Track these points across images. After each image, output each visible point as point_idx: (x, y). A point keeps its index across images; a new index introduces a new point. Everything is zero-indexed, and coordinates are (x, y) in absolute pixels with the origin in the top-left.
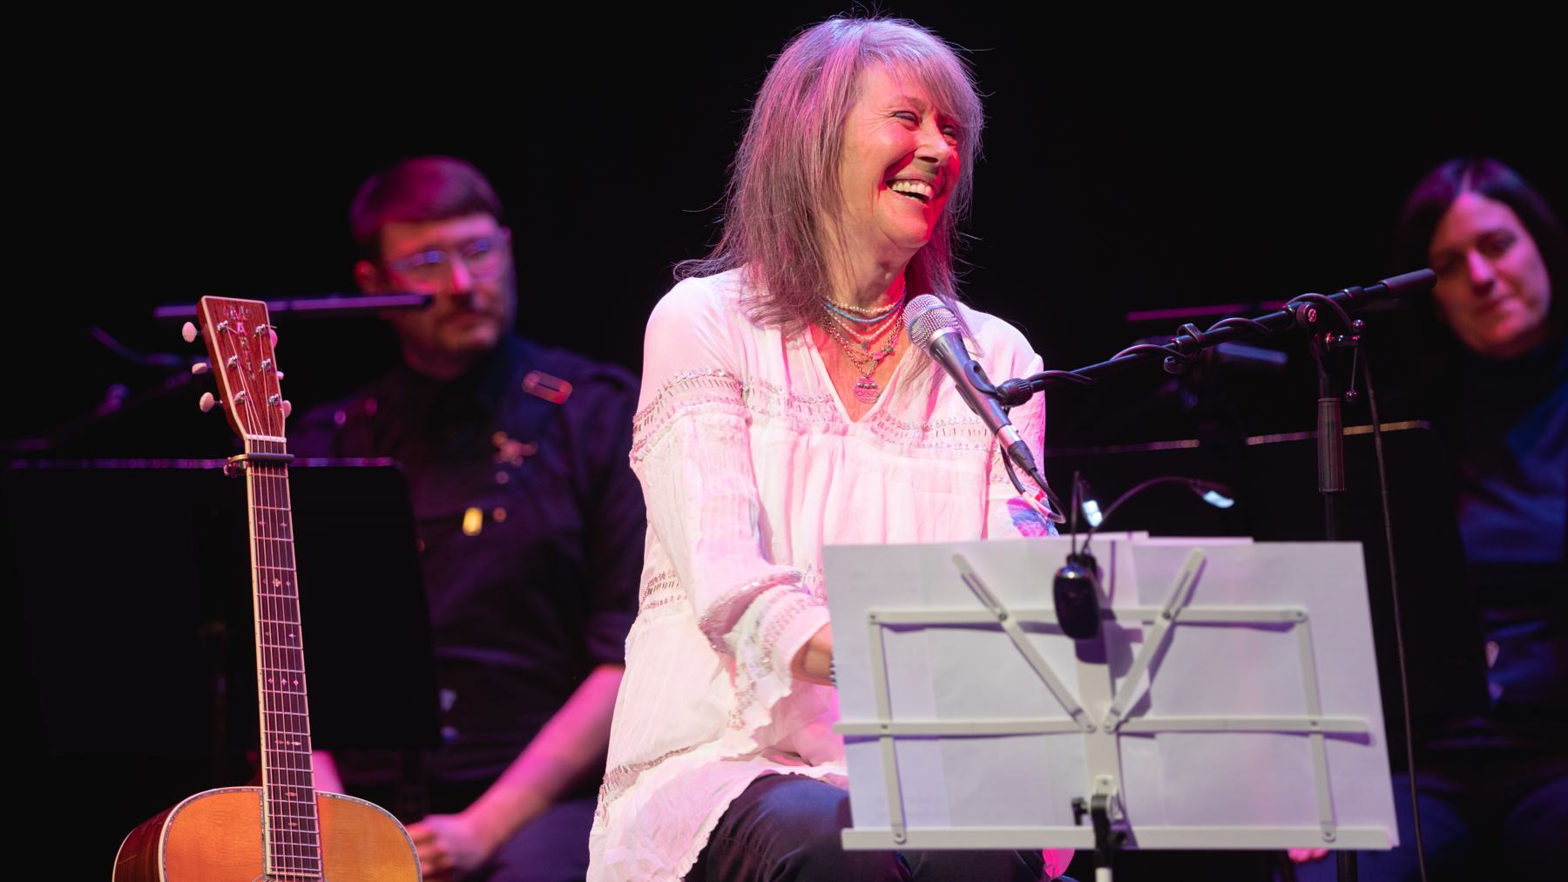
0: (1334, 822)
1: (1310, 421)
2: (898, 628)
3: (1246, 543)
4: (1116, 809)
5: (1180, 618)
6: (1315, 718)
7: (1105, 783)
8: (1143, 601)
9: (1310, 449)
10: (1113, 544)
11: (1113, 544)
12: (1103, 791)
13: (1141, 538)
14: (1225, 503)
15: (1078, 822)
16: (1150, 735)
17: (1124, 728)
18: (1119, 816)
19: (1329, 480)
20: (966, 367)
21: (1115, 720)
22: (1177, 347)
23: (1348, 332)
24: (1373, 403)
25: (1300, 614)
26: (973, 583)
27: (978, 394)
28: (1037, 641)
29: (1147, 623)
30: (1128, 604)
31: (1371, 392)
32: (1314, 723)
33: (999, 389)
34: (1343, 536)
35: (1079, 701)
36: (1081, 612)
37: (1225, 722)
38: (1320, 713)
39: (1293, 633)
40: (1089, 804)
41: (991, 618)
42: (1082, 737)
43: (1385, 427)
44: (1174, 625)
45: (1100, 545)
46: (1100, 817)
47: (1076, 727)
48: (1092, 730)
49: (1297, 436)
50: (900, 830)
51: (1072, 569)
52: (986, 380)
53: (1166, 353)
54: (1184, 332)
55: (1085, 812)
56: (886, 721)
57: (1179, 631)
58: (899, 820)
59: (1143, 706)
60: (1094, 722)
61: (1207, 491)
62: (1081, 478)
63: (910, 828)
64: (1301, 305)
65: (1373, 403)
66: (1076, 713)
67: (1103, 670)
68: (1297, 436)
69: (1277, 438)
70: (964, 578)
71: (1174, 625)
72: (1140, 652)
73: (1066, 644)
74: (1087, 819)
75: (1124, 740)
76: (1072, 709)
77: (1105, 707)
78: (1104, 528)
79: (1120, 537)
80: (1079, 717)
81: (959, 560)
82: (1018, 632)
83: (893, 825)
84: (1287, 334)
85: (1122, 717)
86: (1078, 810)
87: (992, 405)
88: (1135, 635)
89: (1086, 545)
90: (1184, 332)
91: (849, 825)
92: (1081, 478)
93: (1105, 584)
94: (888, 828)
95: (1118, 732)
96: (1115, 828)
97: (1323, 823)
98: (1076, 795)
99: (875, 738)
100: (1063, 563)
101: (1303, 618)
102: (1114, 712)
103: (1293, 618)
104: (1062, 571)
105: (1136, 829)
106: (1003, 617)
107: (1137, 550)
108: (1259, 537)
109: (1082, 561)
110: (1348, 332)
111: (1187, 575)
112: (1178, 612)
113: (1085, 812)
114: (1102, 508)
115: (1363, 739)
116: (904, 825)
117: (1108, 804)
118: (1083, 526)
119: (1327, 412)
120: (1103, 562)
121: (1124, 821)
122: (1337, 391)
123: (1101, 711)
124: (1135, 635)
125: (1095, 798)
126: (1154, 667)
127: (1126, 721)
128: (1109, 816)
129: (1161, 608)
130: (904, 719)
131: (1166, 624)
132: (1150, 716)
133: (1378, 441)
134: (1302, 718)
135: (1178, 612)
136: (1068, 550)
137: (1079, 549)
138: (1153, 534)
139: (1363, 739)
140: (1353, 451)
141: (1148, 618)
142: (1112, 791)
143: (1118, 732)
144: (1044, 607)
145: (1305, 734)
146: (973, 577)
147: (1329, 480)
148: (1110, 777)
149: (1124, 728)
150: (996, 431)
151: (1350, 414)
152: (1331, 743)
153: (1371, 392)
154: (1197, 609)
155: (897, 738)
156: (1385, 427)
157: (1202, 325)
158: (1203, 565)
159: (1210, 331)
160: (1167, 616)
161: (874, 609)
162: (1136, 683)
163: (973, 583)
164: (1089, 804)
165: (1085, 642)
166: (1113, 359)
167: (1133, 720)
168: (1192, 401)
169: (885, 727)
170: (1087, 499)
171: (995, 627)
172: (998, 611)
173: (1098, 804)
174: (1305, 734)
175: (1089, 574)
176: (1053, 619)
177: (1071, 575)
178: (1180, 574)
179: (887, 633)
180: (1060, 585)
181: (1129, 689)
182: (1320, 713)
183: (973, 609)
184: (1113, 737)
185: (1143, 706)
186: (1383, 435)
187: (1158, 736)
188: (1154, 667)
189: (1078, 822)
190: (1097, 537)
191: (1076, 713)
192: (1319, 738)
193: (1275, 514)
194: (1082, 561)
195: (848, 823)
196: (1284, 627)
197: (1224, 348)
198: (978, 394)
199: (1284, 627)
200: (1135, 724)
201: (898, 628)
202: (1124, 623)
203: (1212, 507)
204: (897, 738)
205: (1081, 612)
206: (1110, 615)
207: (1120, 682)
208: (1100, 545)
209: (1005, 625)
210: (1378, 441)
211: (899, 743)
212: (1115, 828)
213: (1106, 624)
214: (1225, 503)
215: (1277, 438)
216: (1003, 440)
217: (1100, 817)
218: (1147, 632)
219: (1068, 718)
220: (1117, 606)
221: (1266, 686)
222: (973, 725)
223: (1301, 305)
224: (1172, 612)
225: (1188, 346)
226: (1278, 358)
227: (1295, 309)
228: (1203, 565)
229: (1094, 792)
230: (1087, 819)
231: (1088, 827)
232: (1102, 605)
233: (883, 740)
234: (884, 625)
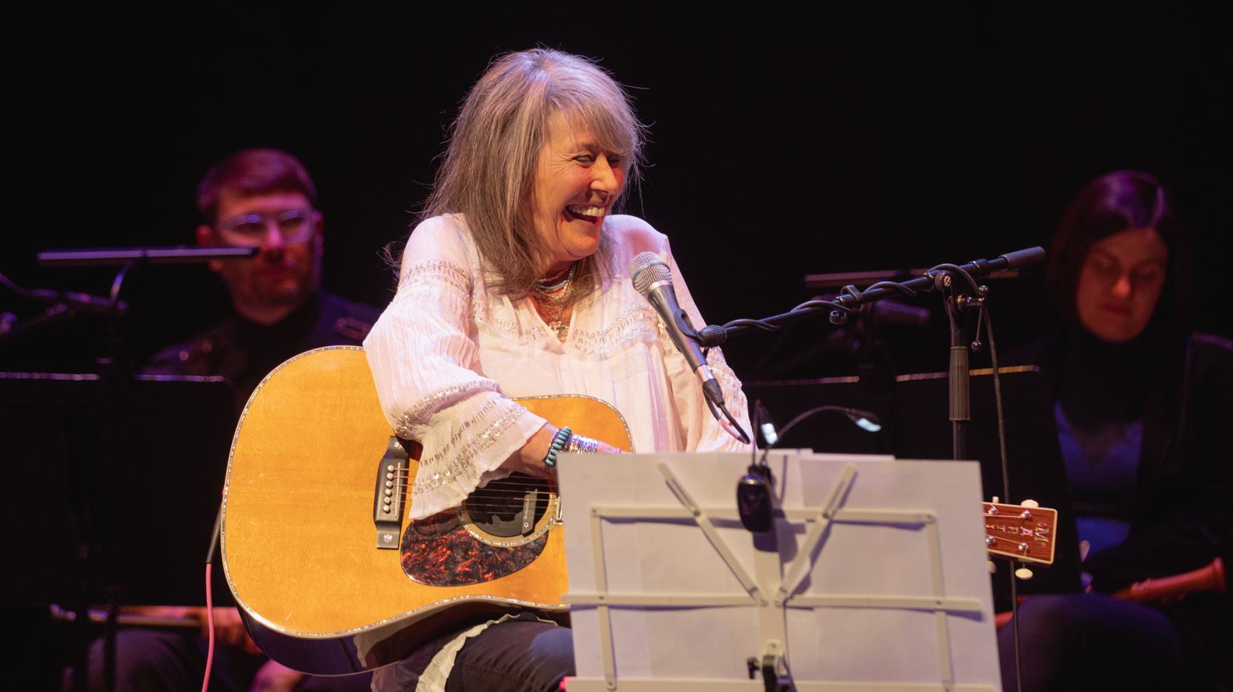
0: (953, 681)
1: (945, 367)
2: (614, 520)
3: (889, 459)
4: (782, 667)
5: (836, 518)
6: (940, 598)
7: (774, 646)
8: (807, 503)
9: (943, 387)
10: (785, 458)
11: (785, 458)
12: (772, 652)
13: (807, 454)
14: (874, 428)
15: (752, 676)
16: (810, 609)
17: (790, 603)
18: (784, 672)
19: (957, 410)
20: (675, 315)
21: (783, 597)
22: (841, 303)
23: (975, 296)
24: (993, 351)
25: (929, 517)
26: (674, 488)
27: (683, 337)
28: (723, 534)
29: (811, 521)
30: (794, 504)
31: (992, 343)
32: (939, 603)
33: (700, 333)
34: (967, 456)
35: (755, 582)
36: (758, 510)
37: (869, 600)
38: (943, 594)
39: (924, 532)
40: (760, 662)
41: (688, 514)
42: (757, 610)
43: (1004, 370)
44: (832, 522)
45: (775, 459)
46: (769, 673)
47: (753, 602)
48: (764, 604)
49: (936, 375)
50: (612, 680)
51: (751, 477)
52: (691, 327)
53: (832, 307)
54: (846, 292)
55: (757, 668)
56: (603, 594)
57: (836, 528)
58: (611, 671)
59: (804, 585)
60: (766, 597)
61: (860, 417)
62: (761, 406)
63: (620, 678)
64: (940, 275)
65: (993, 351)
66: (752, 591)
67: (774, 557)
68: (936, 375)
69: (921, 376)
70: (668, 484)
71: (832, 522)
72: (804, 542)
73: (746, 536)
74: (759, 674)
75: (789, 612)
76: (749, 587)
77: (775, 586)
78: (777, 446)
79: (791, 453)
80: (755, 594)
81: (663, 468)
82: (709, 527)
83: (606, 676)
84: (931, 296)
85: (788, 595)
86: (752, 667)
87: (691, 346)
88: (800, 529)
89: (764, 458)
90: (846, 292)
91: (572, 673)
92: (761, 406)
93: (778, 490)
94: (602, 678)
95: (785, 605)
96: (781, 682)
97: (944, 681)
98: (751, 655)
99: (594, 607)
100: (745, 472)
101: (932, 520)
102: (783, 590)
103: (925, 519)
104: (744, 478)
105: (797, 683)
106: (697, 513)
107: (804, 464)
108: (900, 455)
109: (761, 471)
110: (975, 296)
111: (842, 483)
112: (834, 513)
113: (757, 668)
114: (777, 430)
115: (977, 616)
116: (615, 676)
117: (775, 663)
118: (761, 442)
119: (957, 357)
120: (776, 472)
121: (788, 677)
122: (966, 340)
123: (772, 589)
124: (800, 529)
125: (769, 657)
126: (815, 556)
127: (791, 597)
128: (776, 672)
129: (821, 509)
130: (617, 593)
131: (825, 522)
132: (810, 594)
133: (997, 382)
134: (929, 598)
135: (834, 513)
136: (749, 462)
137: (758, 462)
138: (817, 450)
139: (977, 616)
140: (978, 390)
141: (811, 517)
142: (779, 653)
143: (785, 605)
144: (729, 506)
145: (931, 611)
146: (674, 482)
147: (957, 410)
148: (777, 642)
149: (790, 603)
150: (695, 369)
151: (977, 359)
152: (952, 619)
153: (992, 343)
154: (850, 511)
155: (612, 607)
156: (1004, 370)
157: (861, 288)
158: (855, 476)
159: (867, 291)
160: (825, 516)
161: (596, 504)
162: (799, 567)
163: (674, 488)
164: (760, 662)
165: (760, 535)
166: (794, 311)
167: (797, 597)
168: (856, 345)
169: (601, 598)
170: (766, 422)
171: (690, 522)
172: (693, 509)
173: (768, 663)
174: (931, 611)
175: (764, 481)
176: (736, 517)
177: (751, 482)
178: (836, 483)
179: (604, 523)
180: (743, 491)
181: (794, 572)
182: (943, 594)
183: (673, 507)
184: (781, 610)
185: (804, 585)
186: (1002, 376)
187: (817, 610)
188: (815, 556)
189: (752, 676)
190: (773, 453)
191: (752, 591)
192: (943, 614)
193: (915, 436)
194: (761, 471)
195: (572, 673)
196: (917, 526)
197: (881, 303)
198: (683, 337)
199: (917, 526)
200: (798, 600)
201: (614, 520)
202: (792, 520)
203: (863, 431)
204: (612, 607)
205: (758, 510)
206: (781, 514)
207: (788, 567)
208: (775, 459)
209: (699, 520)
210: (997, 382)
211: (614, 612)
212: (781, 682)
213: (778, 521)
214: (874, 428)
215: (921, 376)
216: (700, 377)
217: (769, 673)
218: (810, 528)
219: (746, 595)
220: (787, 507)
221: (902, 571)
222: (671, 598)
223: (940, 275)
224: (830, 513)
225: (851, 303)
226: (923, 313)
227: (934, 275)
228: (855, 476)
229: (765, 652)
230: (759, 674)
231: (759, 680)
232: (775, 506)
233: (600, 609)
234: (602, 518)
